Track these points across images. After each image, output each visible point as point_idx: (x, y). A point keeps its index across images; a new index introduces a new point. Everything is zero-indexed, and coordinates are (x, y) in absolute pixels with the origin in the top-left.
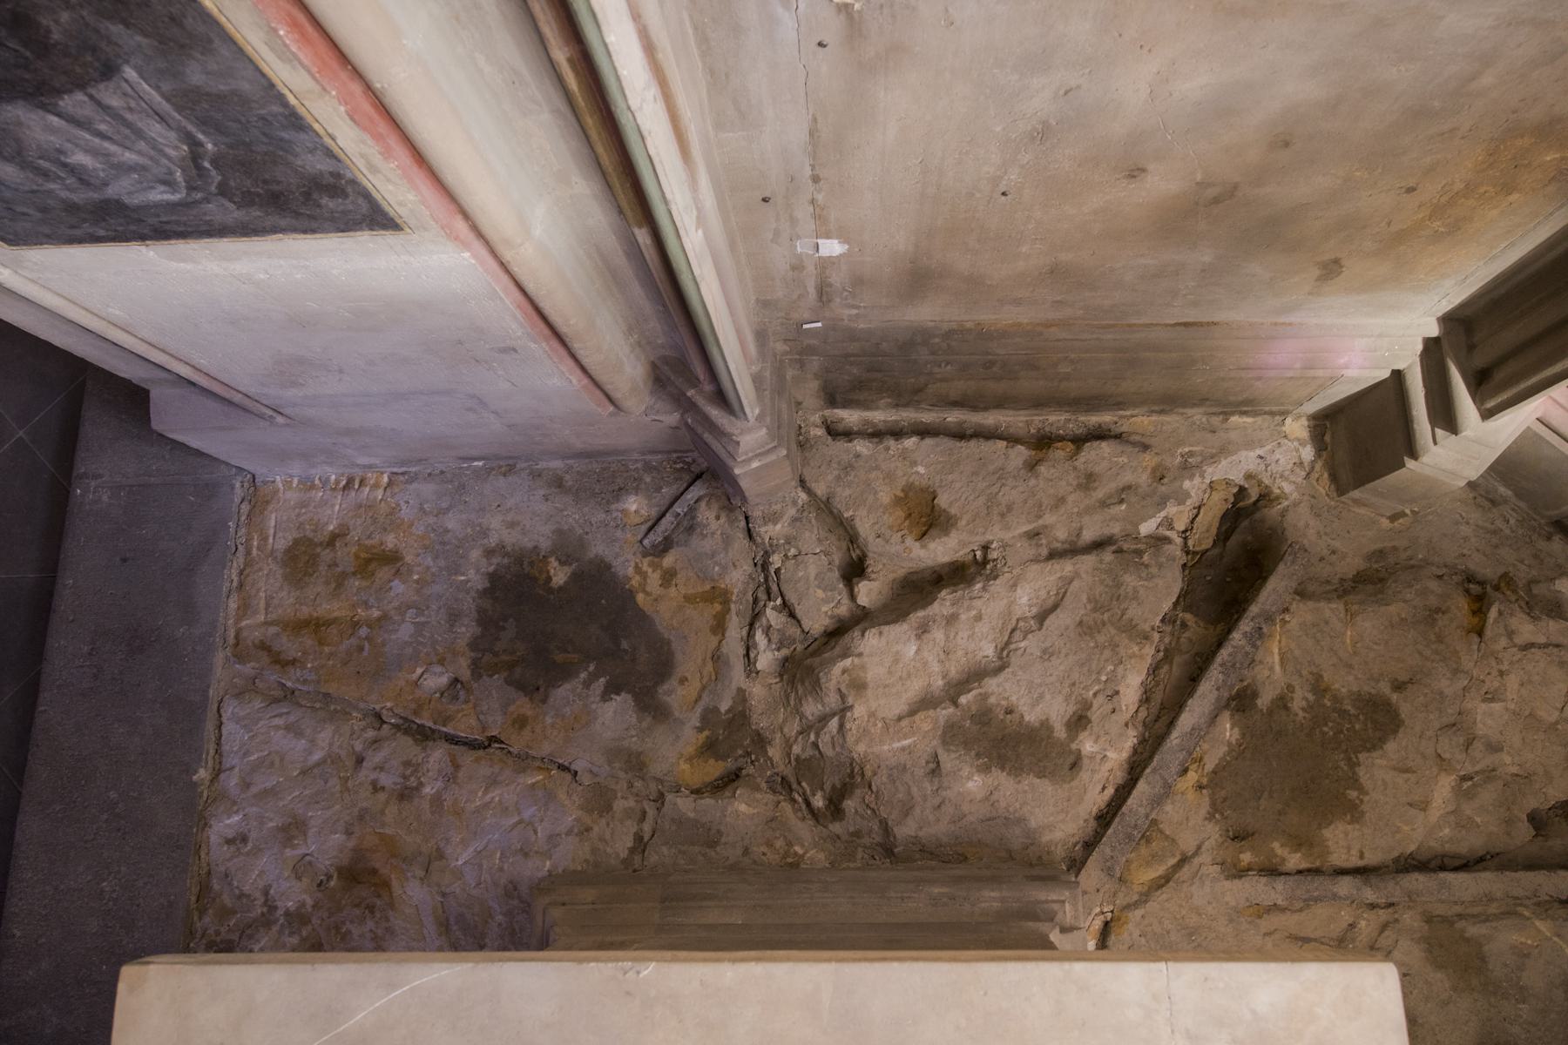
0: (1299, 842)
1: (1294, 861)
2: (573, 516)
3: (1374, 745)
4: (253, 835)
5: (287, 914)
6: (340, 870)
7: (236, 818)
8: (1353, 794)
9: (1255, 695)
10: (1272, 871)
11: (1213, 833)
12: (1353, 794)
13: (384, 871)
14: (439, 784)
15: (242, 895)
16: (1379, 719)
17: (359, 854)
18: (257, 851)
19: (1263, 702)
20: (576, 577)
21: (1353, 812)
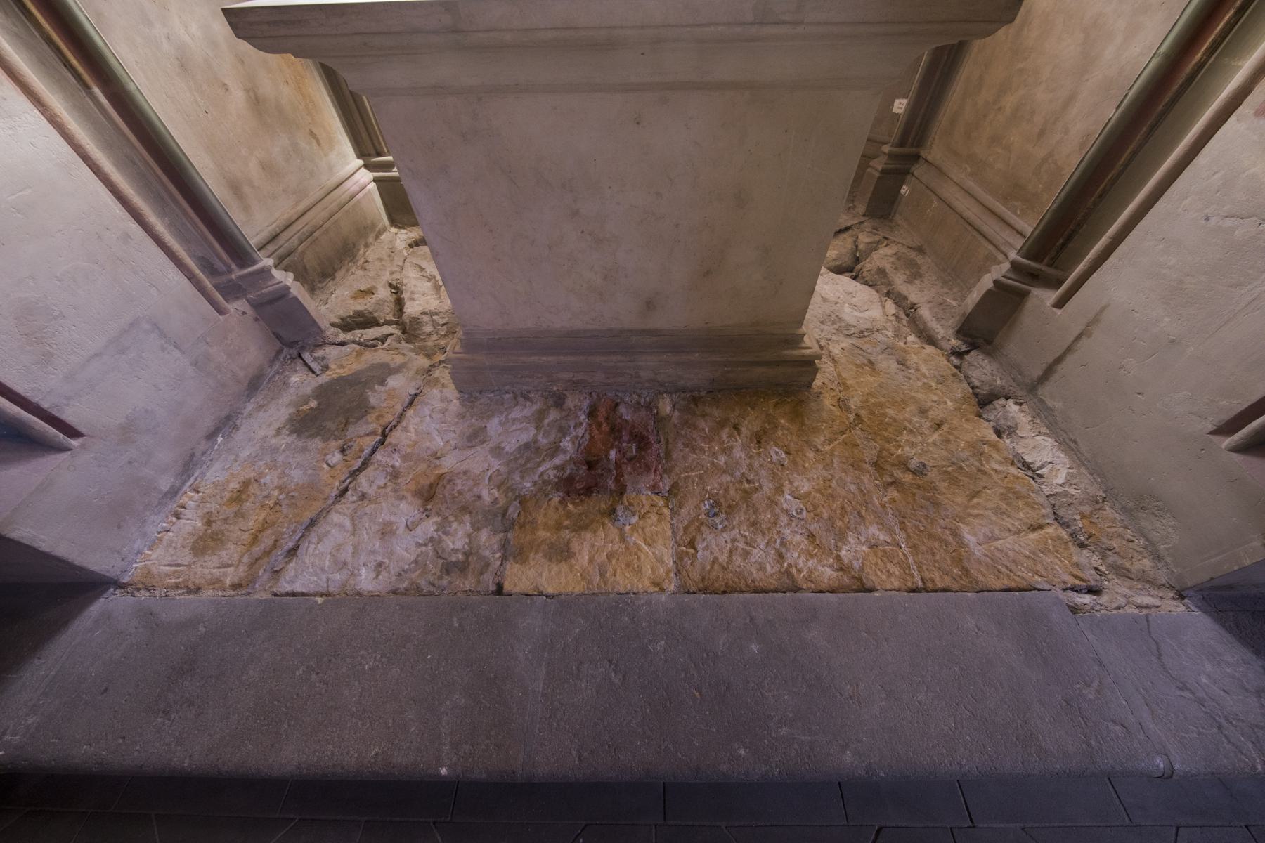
2: (285, 399)
4: (380, 558)
5: (436, 531)
6: (424, 505)
7: (363, 571)
13: (432, 479)
14: (396, 456)
15: (416, 562)
17: (418, 493)
18: (391, 554)
20: (317, 397)
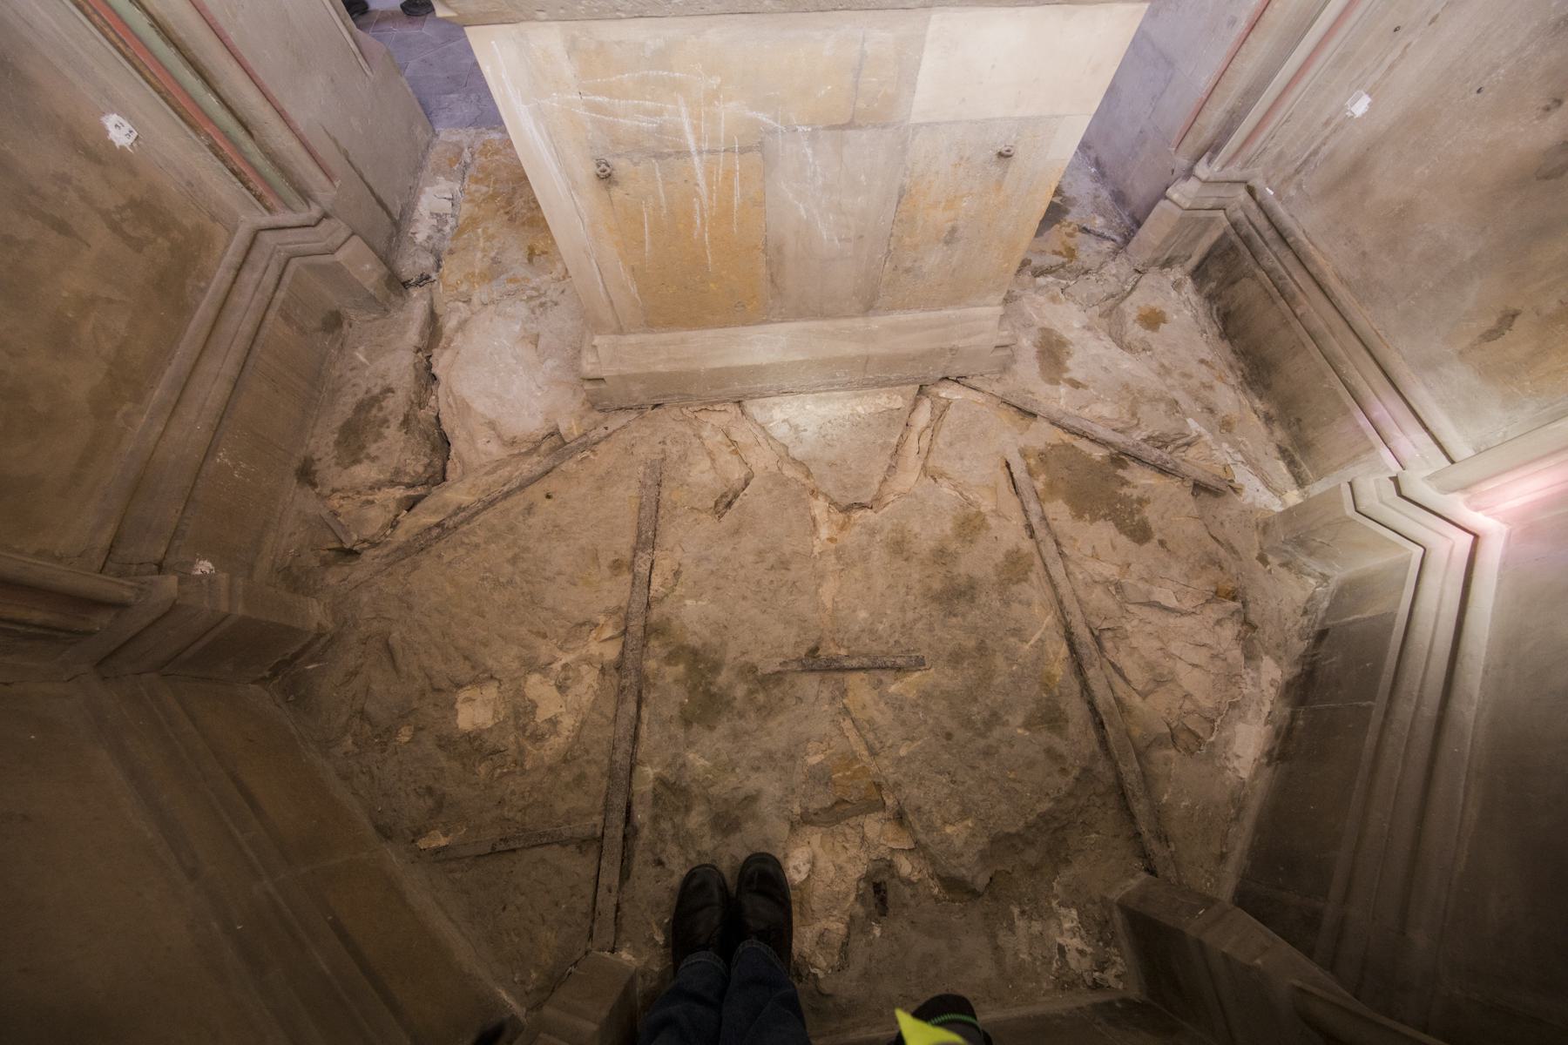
0: (1051, 486)
1: (1039, 485)
3: (1121, 527)
8: (1087, 516)
9: (1124, 468)
10: (1030, 473)
11: (1040, 446)
12: (1087, 516)
16: (1141, 534)
19: (1120, 472)
21: (1079, 515)
